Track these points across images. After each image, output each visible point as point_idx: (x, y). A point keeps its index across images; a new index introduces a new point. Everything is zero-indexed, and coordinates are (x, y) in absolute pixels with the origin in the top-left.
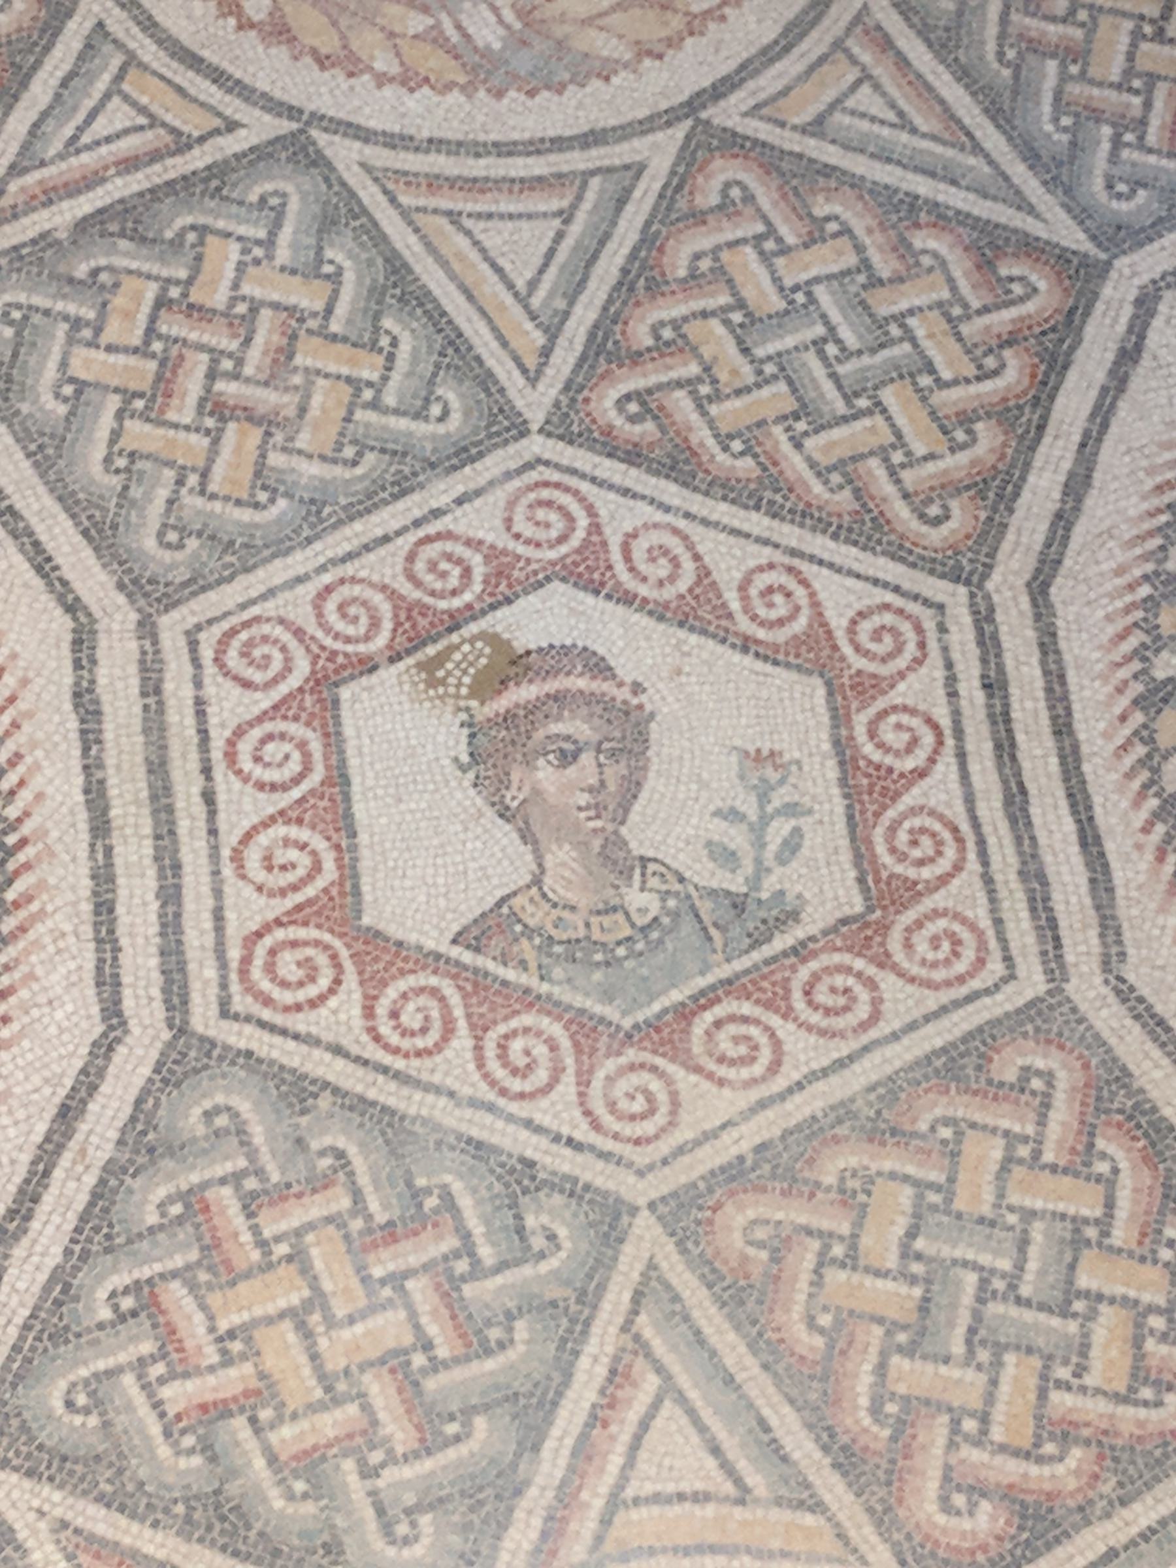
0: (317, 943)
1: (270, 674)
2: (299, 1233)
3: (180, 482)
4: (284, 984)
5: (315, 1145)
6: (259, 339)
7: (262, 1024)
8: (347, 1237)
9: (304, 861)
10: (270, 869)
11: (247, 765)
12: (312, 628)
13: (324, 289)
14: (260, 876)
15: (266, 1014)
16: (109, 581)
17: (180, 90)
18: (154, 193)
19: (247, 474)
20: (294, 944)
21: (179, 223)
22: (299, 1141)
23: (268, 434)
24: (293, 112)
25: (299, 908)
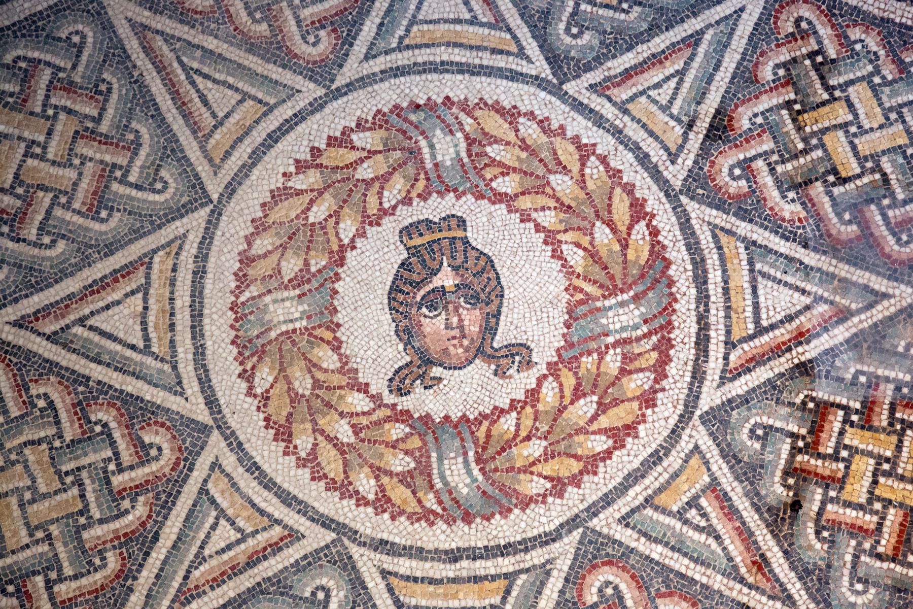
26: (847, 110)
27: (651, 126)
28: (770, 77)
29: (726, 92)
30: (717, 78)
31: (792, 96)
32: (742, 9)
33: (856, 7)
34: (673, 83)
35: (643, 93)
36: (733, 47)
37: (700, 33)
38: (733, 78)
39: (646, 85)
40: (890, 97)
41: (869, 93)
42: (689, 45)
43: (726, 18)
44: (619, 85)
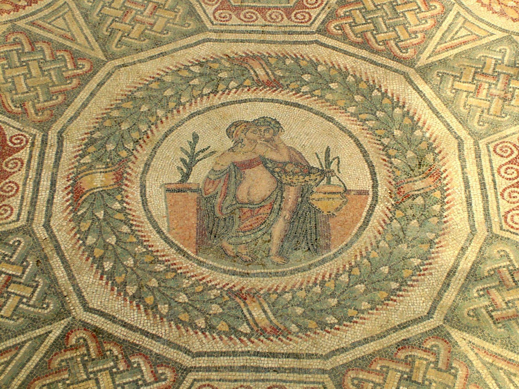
1: (507, 154)
3: (482, 111)
10: (510, 197)
11: (503, 174)
14: (508, 199)
15: (512, 230)
17: (478, 26)
21: (479, 55)
26: (95, 384)
29: (31, 373)
31: (67, 376)
33: (111, 334)
36: (40, 350)
37: (25, 342)
38: (36, 366)
40: (120, 379)
42: (16, 349)
43: (40, 336)
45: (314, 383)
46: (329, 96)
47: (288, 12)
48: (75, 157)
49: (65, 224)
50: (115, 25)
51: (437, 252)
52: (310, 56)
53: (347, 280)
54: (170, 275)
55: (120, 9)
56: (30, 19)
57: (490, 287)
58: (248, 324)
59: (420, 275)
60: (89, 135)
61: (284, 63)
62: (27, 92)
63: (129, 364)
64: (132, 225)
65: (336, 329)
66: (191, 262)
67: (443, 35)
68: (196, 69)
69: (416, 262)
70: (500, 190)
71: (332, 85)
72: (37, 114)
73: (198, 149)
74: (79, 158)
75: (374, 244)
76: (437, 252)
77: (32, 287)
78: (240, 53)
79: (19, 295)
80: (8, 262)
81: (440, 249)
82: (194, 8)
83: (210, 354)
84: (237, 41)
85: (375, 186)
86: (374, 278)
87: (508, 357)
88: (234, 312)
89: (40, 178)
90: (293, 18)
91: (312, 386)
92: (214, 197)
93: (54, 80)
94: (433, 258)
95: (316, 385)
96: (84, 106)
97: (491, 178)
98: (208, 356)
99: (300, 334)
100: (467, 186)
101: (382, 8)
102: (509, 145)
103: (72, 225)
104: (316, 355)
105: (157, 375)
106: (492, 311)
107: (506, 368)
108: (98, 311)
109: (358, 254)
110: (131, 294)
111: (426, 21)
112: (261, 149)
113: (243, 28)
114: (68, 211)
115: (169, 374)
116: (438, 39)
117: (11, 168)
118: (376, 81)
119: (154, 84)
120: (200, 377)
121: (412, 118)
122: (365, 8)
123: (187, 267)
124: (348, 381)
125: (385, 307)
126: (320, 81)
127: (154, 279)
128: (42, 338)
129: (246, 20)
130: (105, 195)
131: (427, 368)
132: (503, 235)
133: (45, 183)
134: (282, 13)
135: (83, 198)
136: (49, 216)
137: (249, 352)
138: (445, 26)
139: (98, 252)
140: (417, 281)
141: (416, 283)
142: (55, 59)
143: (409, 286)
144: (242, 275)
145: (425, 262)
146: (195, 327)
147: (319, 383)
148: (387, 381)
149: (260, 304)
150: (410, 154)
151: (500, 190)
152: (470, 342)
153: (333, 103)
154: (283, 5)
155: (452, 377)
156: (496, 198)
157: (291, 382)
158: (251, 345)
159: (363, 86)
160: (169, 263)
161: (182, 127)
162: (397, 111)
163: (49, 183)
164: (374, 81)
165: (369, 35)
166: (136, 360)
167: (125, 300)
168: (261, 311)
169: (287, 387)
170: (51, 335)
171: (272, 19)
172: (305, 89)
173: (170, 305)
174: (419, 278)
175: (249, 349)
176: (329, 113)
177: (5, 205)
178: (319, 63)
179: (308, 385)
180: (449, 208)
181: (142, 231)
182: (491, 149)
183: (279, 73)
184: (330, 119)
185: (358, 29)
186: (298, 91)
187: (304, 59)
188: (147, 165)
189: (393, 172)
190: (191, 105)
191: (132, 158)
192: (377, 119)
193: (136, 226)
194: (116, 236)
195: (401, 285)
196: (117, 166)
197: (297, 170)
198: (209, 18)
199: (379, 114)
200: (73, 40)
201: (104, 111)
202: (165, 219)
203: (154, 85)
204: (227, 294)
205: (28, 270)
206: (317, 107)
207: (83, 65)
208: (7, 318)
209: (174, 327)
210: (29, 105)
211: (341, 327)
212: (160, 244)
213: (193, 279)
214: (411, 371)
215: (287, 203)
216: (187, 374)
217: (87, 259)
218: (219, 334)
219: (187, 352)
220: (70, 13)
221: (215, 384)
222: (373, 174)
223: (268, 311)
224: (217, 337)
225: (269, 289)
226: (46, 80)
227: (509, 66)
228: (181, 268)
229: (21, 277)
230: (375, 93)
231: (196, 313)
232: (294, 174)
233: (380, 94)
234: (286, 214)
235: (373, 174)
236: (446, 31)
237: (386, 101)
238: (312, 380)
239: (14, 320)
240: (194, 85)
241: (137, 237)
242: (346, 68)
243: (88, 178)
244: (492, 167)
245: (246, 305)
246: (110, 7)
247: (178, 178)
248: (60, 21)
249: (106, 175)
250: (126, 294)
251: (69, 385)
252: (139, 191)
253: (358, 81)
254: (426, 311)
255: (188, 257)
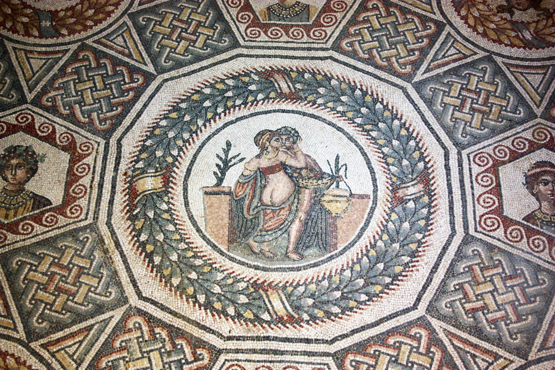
0: (494, 218)
2: (492, 276)
4: (488, 226)
5: (495, 258)
6: (482, 96)
7: (483, 234)
8: (502, 278)
9: (492, 202)
11: (480, 182)
12: (493, 155)
13: (495, 87)
14: (483, 204)
15: (484, 232)
16: (452, 143)
17: (465, 46)
18: (460, 66)
19: (479, 124)
20: (490, 218)
22: (492, 258)
23: (483, 116)
24: (488, 51)
25: (491, 211)
27: (63, 363)
28: (118, 346)
30: (96, 345)
31: (126, 355)
32: (112, 317)
34: (77, 346)
35: (62, 349)
37: (93, 325)
38: (103, 345)
39: (65, 345)
41: (159, 356)
43: (105, 320)
44: (54, 345)
45: (320, 364)
46: (340, 108)
47: (308, 29)
48: (131, 162)
49: (123, 222)
50: (166, 42)
51: (424, 251)
52: (325, 70)
53: (350, 275)
54: (206, 269)
55: (169, 27)
56: (96, 38)
57: (465, 283)
58: (269, 313)
59: (408, 271)
60: (142, 143)
61: (303, 77)
62: (93, 104)
63: (174, 345)
64: (177, 224)
65: (339, 318)
66: (224, 258)
67: (436, 52)
68: (230, 82)
69: (406, 259)
70: (476, 196)
71: (343, 98)
72: (101, 124)
73: (230, 156)
74: (134, 163)
75: (373, 243)
76: (424, 251)
77: (98, 277)
78: (268, 68)
79: (88, 285)
80: (79, 256)
81: (426, 248)
82: (229, 26)
83: (238, 339)
84: (264, 56)
85: (375, 191)
86: (371, 274)
87: (475, 343)
88: (257, 302)
89: (103, 181)
90: (312, 35)
91: (319, 366)
92: (243, 199)
93: (115, 92)
94: (420, 256)
95: (322, 366)
96: (139, 115)
97: (470, 185)
98: (237, 340)
99: (310, 322)
100: (450, 192)
101: (386, 27)
102: (486, 155)
103: (129, 222)
104: (323, 340)
105: (196, 356)
106: (464, 303)
107: (473, 352)
108: (150, 299)
109: (360, 252)
110: (175, 285)
111: (423, 41)
112: (282, 157)
113: (270, 44)
114: (125, 211)
115: (206, 355)
116: (432, 57)
117: (80, 173)
118: (380, 95)
119: (195, 95)
120: (229, 358)
121: (407, 129)
122: (372, 27)
123: (220, 262)
124: (347, 363)
125: (379, 299)
126: (333, 94)
127: (194, 273)
128: (106, 322)
129: (272, 36)
130: (155, 197)
131: (410, 352)
132: (478, 237)
133: (107, 186)
134: (303, 30)
135: (137, 199)
136: (110, 214)
137: (269, 337)
138: (437, 45)
139: (150, 248)
140: (406, 276)
141: (405, 278)
142: (116, 74)
143: (399, 280)
144: (265, 269)
145: (413, 260)
146: (226, 315)
147: (325, 364)
148: (379, 363)
149: (279, 295)
150: (405, 162)
151: (476, 196)
152: (445, 330)
153: (343, 114)
154: (304, 23)
155: (430, 360)
156: (474, 203)
157: (302, 363)
158: (271, 331)
159: (368, 99)
160: (206, 258)
161: (217, 135)
162: (396, 122)
163: (111, 185)
164: (377, 95)
165: (375, 52)
166: (180, 342)
167: (171, 290)
168: (280, 302)
169: (299, 368)
170: (113, 319)
171: (294, 36)
172: (320, 101)
173: (206, 295)
174: (408, 273)
175: (270, 335)
176: (341, 123)
177: (76, 206)
178: (332, 77)
179: (316, 366)
180: (435, 211)
181: (184, 230)
182: (471, 159)
183: (298, 86)
184: (339, 129)
185: (366, 46)
186: (314, 103)
187: (320, 74)
188: (189, 171)
189: (391, 179)
190: (225, 115)
191: (177, 163)
192: (379, 130)
193: (179, 225)
194: (164, 234)
195: (393, 280)
196: (165, 171)
197: (312, 175)
198: (242, 36)
199: (381, 125)
200: (130, 56)
201: (155, 121)
202: (203, 219)
203: (195, 97)
204: (252, 287)
205: (94, 263)
206: (330, 117)
207: (138, 79)
208: (80, 304)
209: (209, 314)
210: (95, 115)
211: (343, 316)
212: (198, 242)
213: (226, 272)
214: (398, 355)
215: (302, 205)
216: (220, 355)
217: (141, 254)
218: (245, 321)
219: (220, 336)
220: (128, 32)
221: (242, 364)
222: (374, 180)
223: (286, 302)
224: (244, 323)
225: (287, 282)
226: (107, 93)
227: (488, 83)
228: (215, 263)
229: (90, 269)
230: (379, 106)
231: (227, 302)
232: (309, 179)
233: (382, 107)
234: (302, 215)
235: (374, 180)
236: (438, 50)
237: (387, 114)
238: (319, 362)
239: (84, 306)
240: (229, 97)
241: (180, 234)
242: (354, 82)
243: (141, 181)
244: (471, 175)
245: (268, 296)
246: (160, 25)
247: (215, 181)
248: (120, 39)
249: (156, 178)
250: (172, 285)
251: (127, 362)
252: (182, 194)
253: (365, 94)
254: (413, 303)
255: (222, 253)
